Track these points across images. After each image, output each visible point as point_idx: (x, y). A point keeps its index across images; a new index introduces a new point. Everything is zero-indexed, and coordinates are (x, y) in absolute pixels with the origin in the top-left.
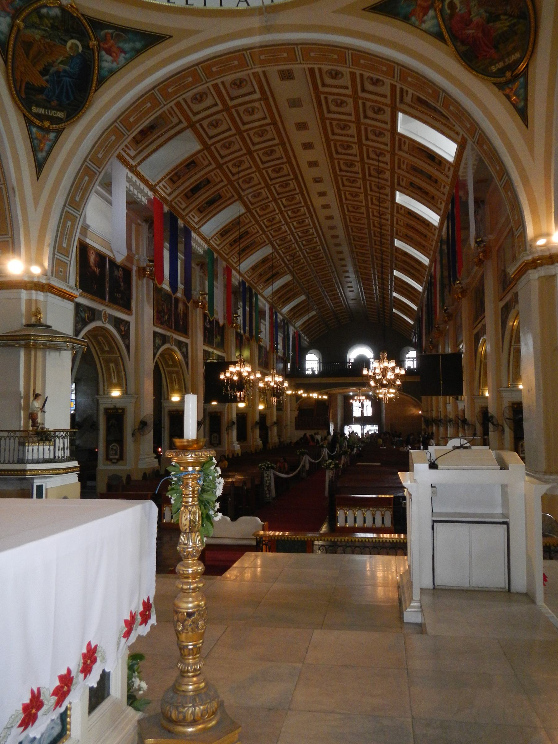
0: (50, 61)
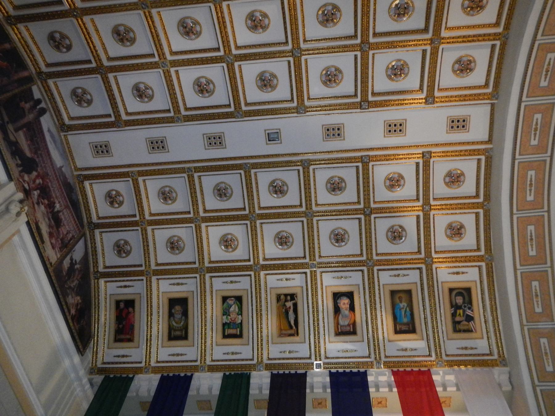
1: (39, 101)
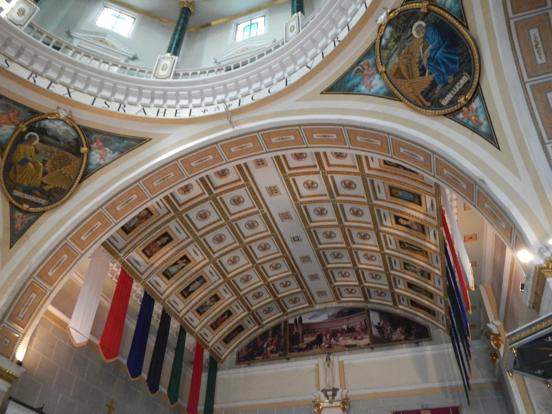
0: (417, 60)
1: (296, 320)
